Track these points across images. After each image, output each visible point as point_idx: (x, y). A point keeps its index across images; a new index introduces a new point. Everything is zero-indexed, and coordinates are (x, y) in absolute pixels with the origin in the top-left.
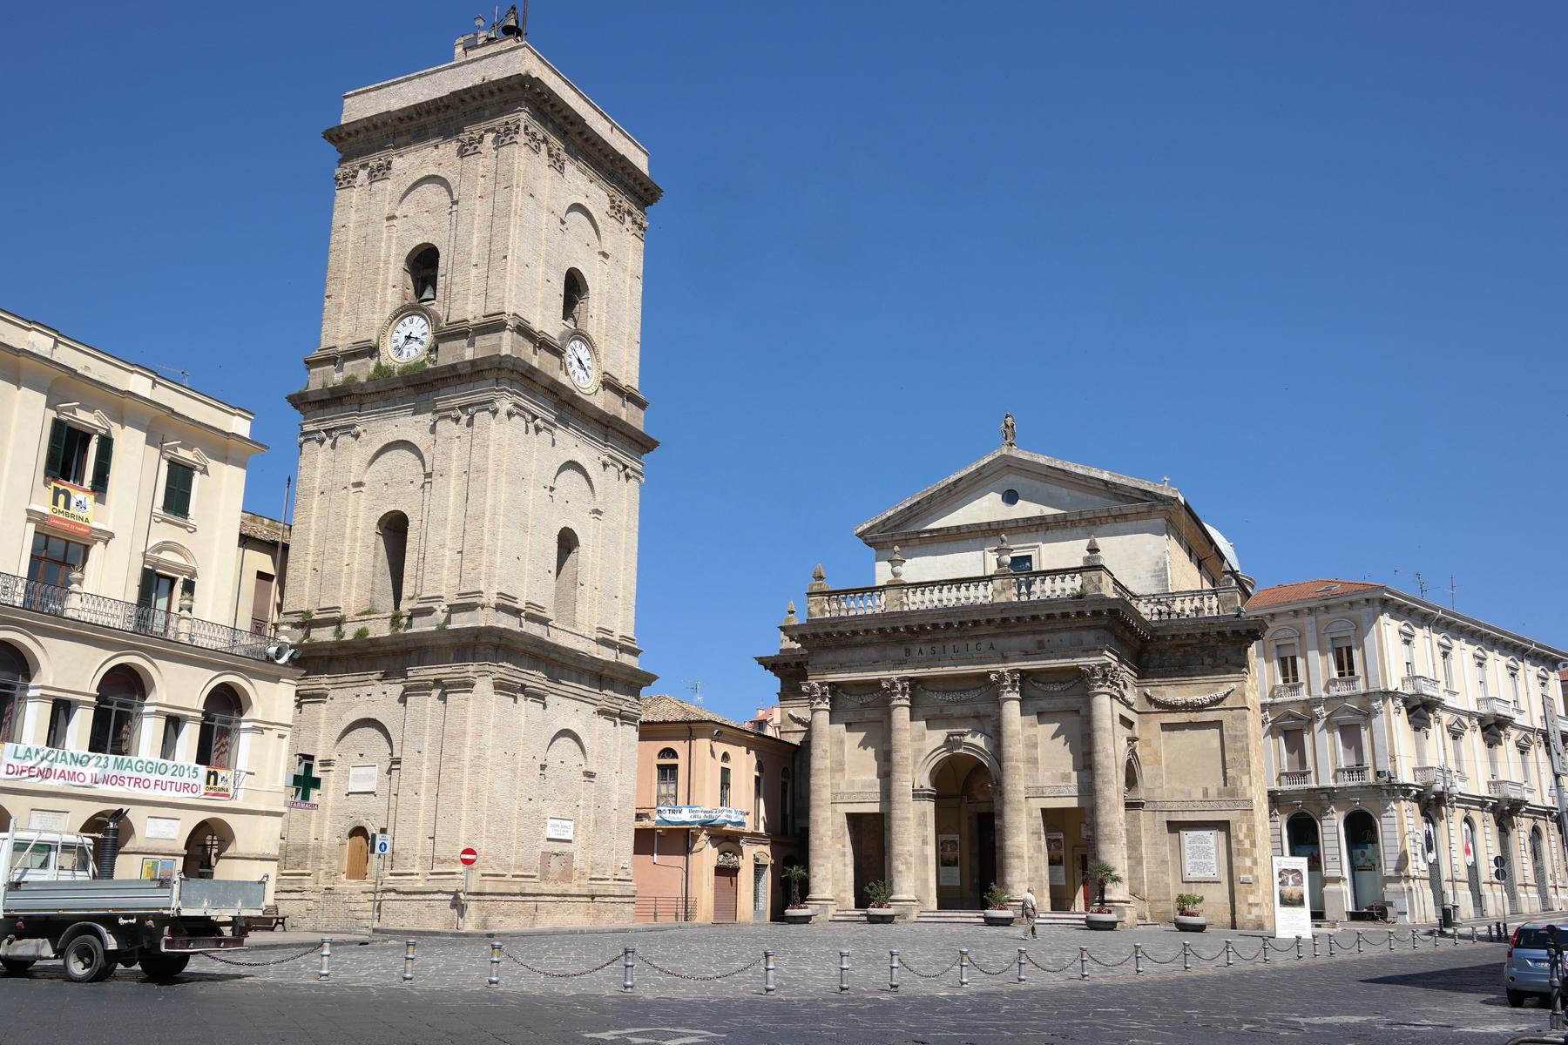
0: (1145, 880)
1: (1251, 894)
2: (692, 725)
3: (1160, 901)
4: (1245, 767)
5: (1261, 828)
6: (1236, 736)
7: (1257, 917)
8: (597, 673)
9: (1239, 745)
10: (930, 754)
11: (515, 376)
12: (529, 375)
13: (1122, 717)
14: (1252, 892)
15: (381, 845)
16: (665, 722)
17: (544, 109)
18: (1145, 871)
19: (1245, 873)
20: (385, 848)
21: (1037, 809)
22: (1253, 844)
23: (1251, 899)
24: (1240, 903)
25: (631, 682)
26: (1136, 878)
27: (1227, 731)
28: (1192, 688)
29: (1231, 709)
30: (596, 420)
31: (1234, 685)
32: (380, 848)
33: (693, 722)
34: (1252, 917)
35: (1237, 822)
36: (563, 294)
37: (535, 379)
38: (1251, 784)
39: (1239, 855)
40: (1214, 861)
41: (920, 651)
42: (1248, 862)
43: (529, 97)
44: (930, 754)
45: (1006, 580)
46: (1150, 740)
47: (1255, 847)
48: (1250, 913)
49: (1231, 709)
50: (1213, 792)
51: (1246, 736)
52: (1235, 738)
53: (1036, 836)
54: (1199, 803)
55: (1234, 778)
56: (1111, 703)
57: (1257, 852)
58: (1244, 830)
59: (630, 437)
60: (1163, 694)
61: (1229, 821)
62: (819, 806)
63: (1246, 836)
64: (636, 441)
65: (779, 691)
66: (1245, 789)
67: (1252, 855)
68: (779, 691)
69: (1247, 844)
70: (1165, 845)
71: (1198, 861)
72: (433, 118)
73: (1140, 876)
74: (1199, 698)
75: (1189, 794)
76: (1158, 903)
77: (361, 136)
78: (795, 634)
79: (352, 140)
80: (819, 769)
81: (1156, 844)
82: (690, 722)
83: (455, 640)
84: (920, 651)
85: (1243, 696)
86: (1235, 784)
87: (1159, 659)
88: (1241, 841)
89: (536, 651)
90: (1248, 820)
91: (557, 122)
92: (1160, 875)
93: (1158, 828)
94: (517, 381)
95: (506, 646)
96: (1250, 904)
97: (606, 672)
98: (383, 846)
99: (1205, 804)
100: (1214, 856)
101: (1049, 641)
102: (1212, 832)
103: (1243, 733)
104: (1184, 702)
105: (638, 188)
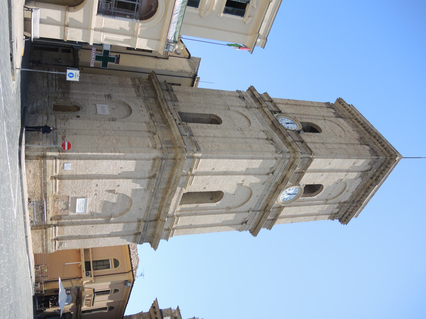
2: (131, 272)
8: (159, 218)
11: (292, 160)
12: (292, 167)
15: (72, 74)
16: (131, 259)
17: (382, 167)
20: (70, 77)
25: (153, 237)
30: (268, 205)
32: (71, 73)
33: (133, 273)
36: (315, 184)
37: (291, 170)
43: (388, 159)
59: (259, 222)
64: (257, 226)
65: (143, 312)
68: (143, 312)
72: (363, 129)
77: (344, 109)
79: (342, 106)
82: (132, 271)
83: (176, 139)
89: (172, 183)
91: (377, 174)
94: (289, 162)
95: (176, 163)
97: (160, 222)
98: (71, 75)
105: (348, 214)
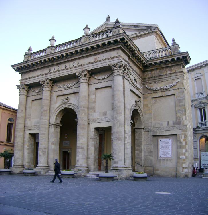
0: (143, 158)
1: (184, 163)
3: (148, 166)
4: (184, 112)
5: (190, 138)
6: (180, 100)
7: (186, 172)
9: (181, 104)
10: (56, 109)
13: (131, 90)
14: (184, 163)
18: (143, 155)
19: (182, 155)
21: (93, 128)
22: (186, 143)
23: (184, 166)
24: (179, 167)
26: (139, 158)
27: (177, 98)
28: (163, 83)
29: (178, 89)
31: (179, 80)
34: (184, 173)
35: (180, 134)
38: (186, 119)
39: (180, 148)
40: (170, 151)
41: (54, 69)
42: (184, 151)
44: (56, 109)
45: (85, 38)
46: (147, 105)
47: (187, 144)
48: (183, 171)
49: (178, 89)
50: (171, 123)
51: (184, 99)
52: (180, 101)
53: (92, 140)
54: (165, 128)
55: (179, 117)
56: (124, 84)
57: (187, 147)
58: (183, 136)
60: (152, 86)
61: (177, 134)
62: (17, 131)
63: (184, 140)
66: (184, 121)
67: (185, 148)
69: (184, 143)
70: (151, 145)
71: (164, 151)
73: (141, 157)
74: (166, 86)
75: (162, 124)
76: (148, 168)
78: (16, 67)
80: (19, 117)
81: (148, 145)
84: (54, 69)
85: (183, 84)
86: (180, 119)
87: (151, 74)
88: (181, 142)
90: (185, 134)
92: (149, 157)
93: (149, 138)
96: (183, 168)
99: (168, 128)
100: (170, 149)
101: (99, 57)
102: (170, 139)
103: (183, 98)
104: (160, 88)
